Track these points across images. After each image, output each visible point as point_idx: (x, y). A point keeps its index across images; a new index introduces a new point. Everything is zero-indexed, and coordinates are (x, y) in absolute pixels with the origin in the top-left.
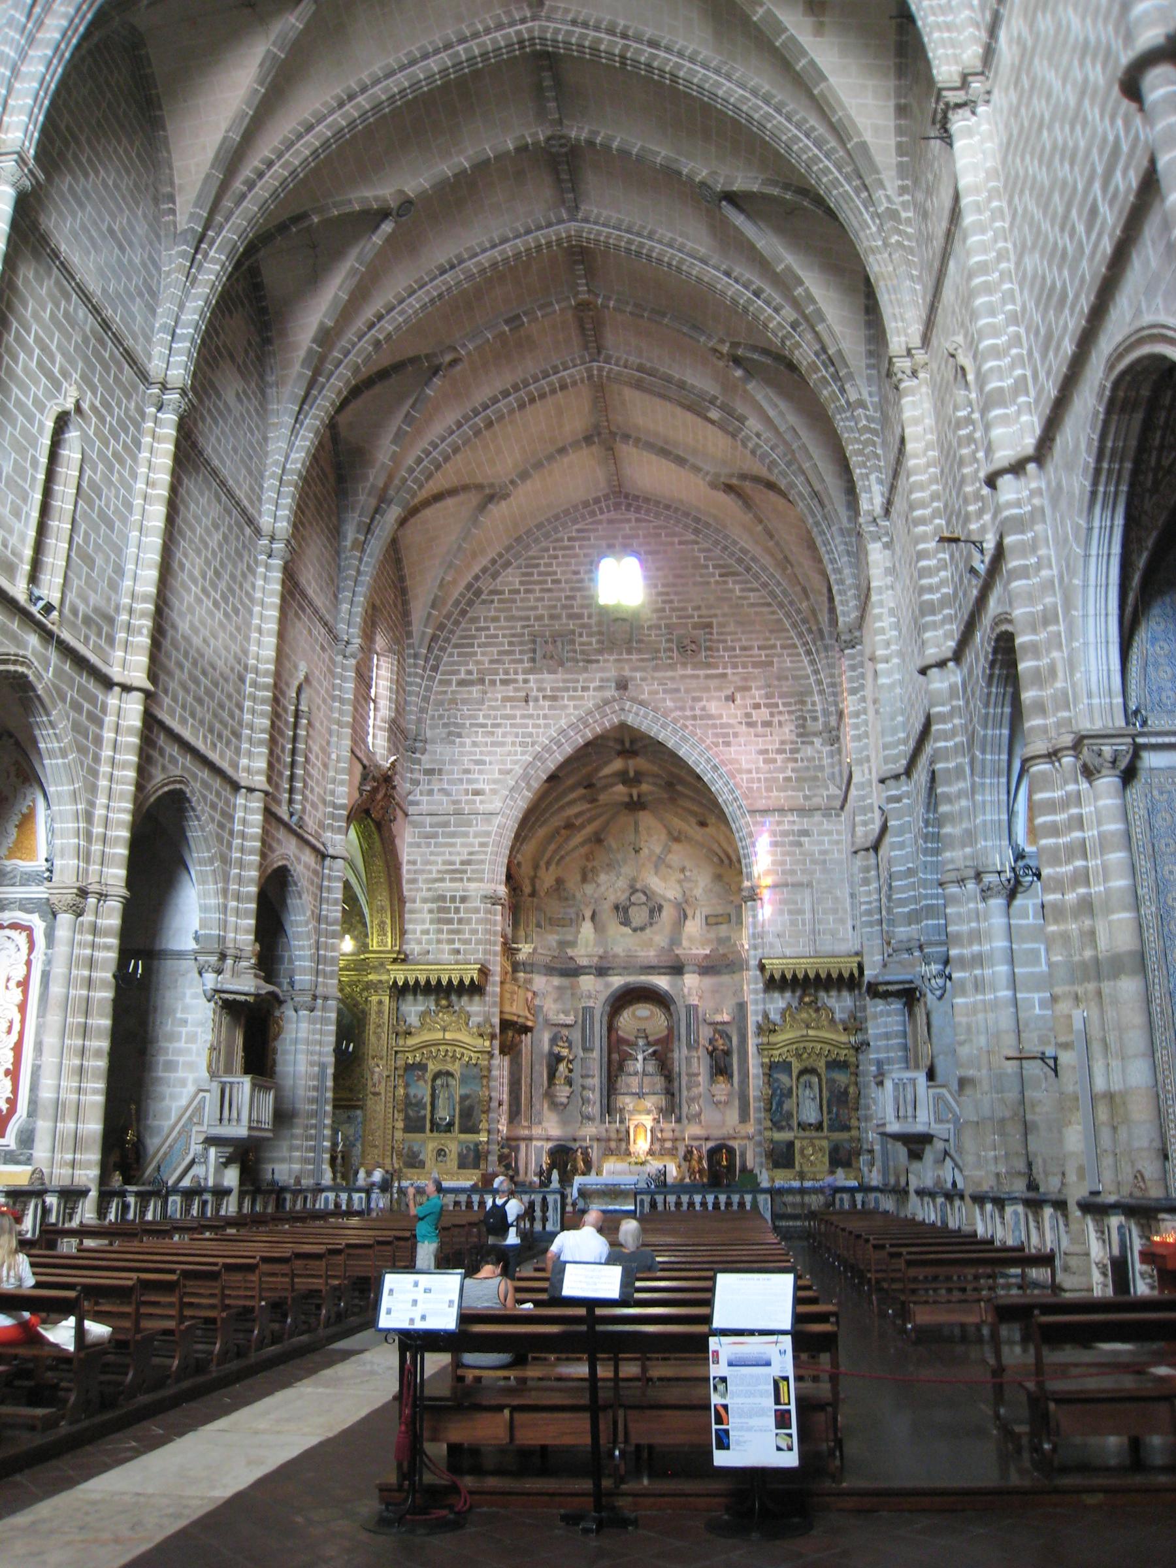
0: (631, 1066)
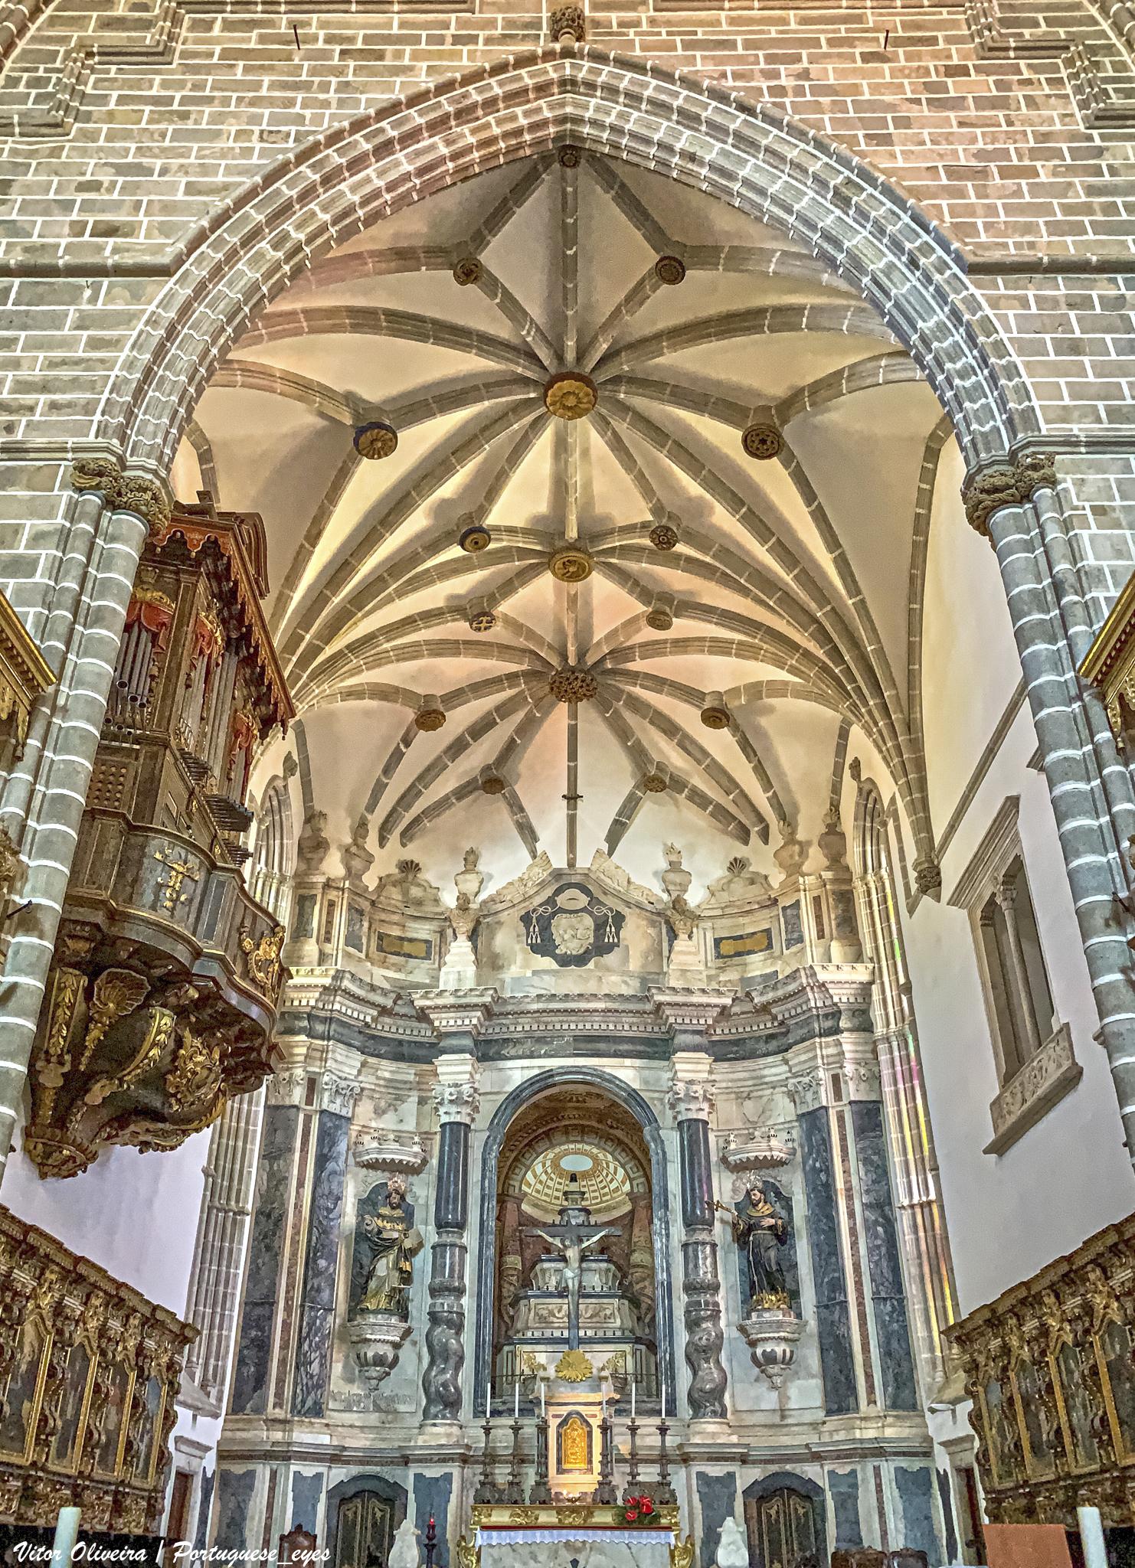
0: (550, 1275)
